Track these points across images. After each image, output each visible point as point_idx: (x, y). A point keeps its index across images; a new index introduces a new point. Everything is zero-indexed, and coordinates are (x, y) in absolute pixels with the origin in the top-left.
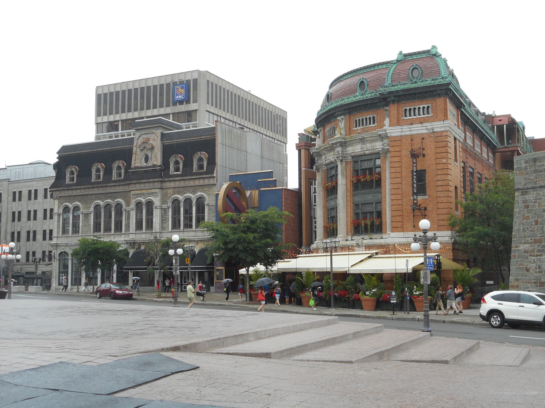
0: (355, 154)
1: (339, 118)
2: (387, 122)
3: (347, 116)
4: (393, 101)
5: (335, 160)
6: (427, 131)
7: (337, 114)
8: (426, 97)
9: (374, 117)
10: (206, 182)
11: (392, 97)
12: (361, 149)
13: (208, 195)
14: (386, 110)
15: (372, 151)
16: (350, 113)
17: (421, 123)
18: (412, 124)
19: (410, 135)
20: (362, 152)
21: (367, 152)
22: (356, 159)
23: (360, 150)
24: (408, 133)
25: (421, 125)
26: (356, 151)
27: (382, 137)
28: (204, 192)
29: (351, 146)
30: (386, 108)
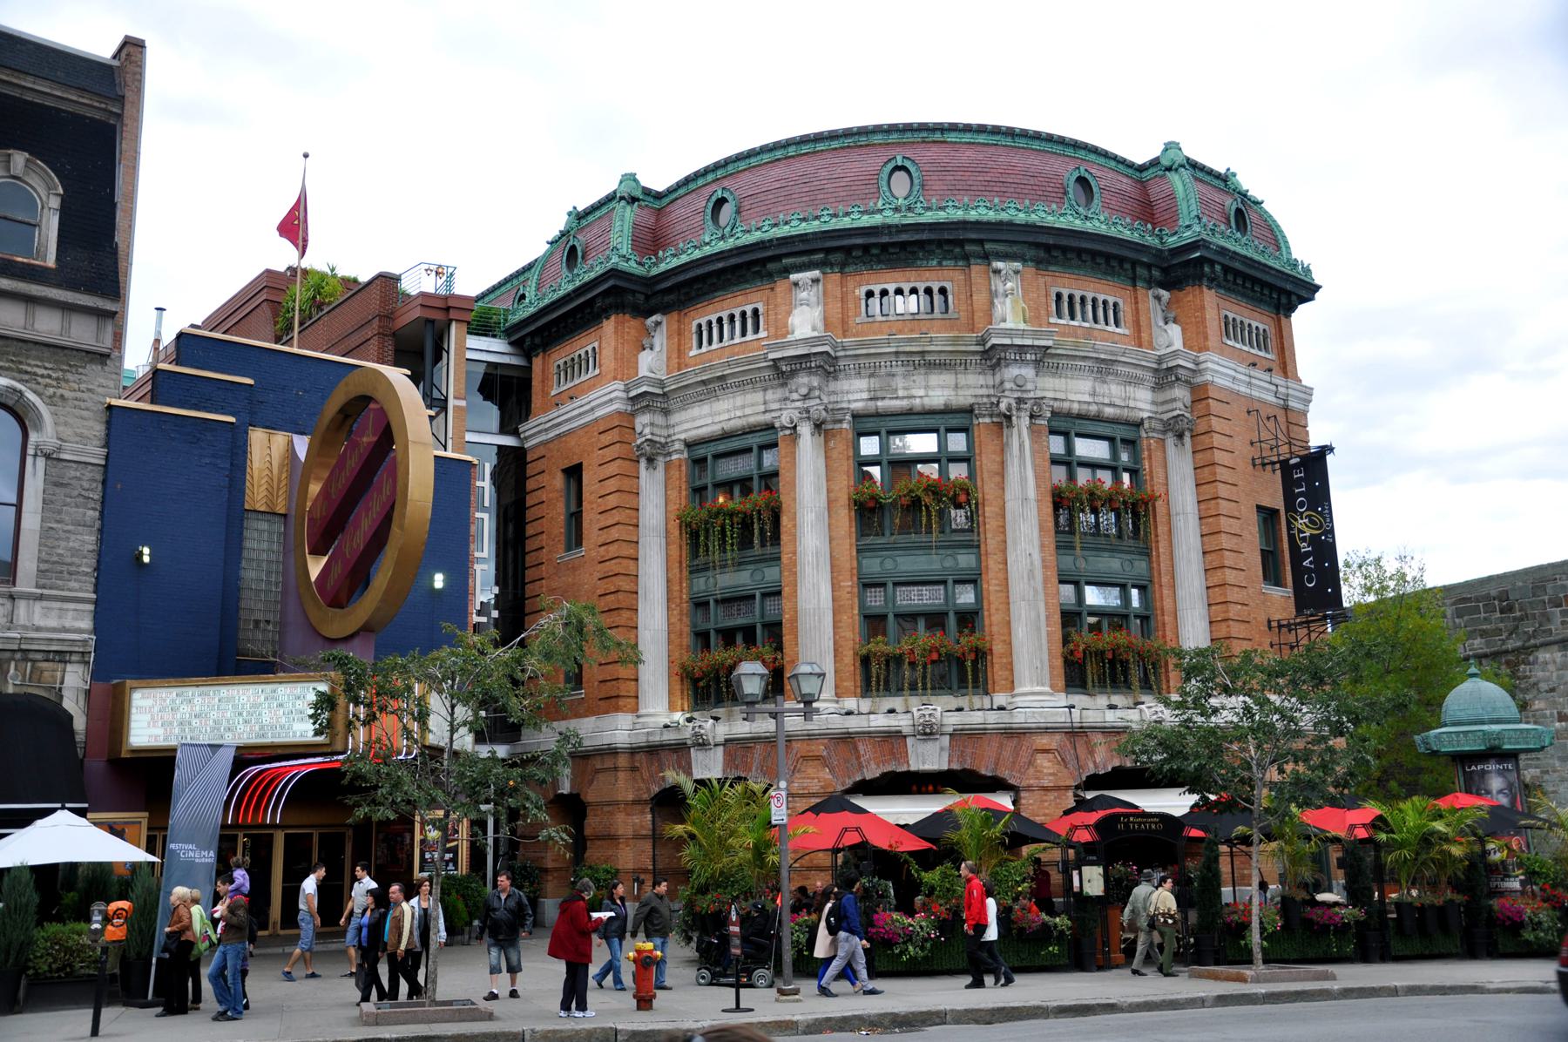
0: (1066, 405)
1: (1000, 265)
2: (1174, 336)
3: (1030, 271)
4: (1213, 282)
5: (1009, 408)
6: (1271, 398)
7: (988, 246)
8: (1261, 301)
9: (1115, 305)
10: (47, 325)
11: (1218, 268)
12: (1094, 394)
13: (51, 401)
14: (1158, 298)
15: (1125, 413)
16: (1039, 263)
17: (1270, 370)
18: (1254, 365)
19: (1251, 398)
20: (1093, 408)
21: (1109, 411)
22: (1067, 424)
23: (1087, 398)
24: (1243, 389)
25: (1266, 376)
26: (1072, 397)
27: (1164, 376)
28: (30, 378)
29: (1054, 375)
30: (1165, 294)
